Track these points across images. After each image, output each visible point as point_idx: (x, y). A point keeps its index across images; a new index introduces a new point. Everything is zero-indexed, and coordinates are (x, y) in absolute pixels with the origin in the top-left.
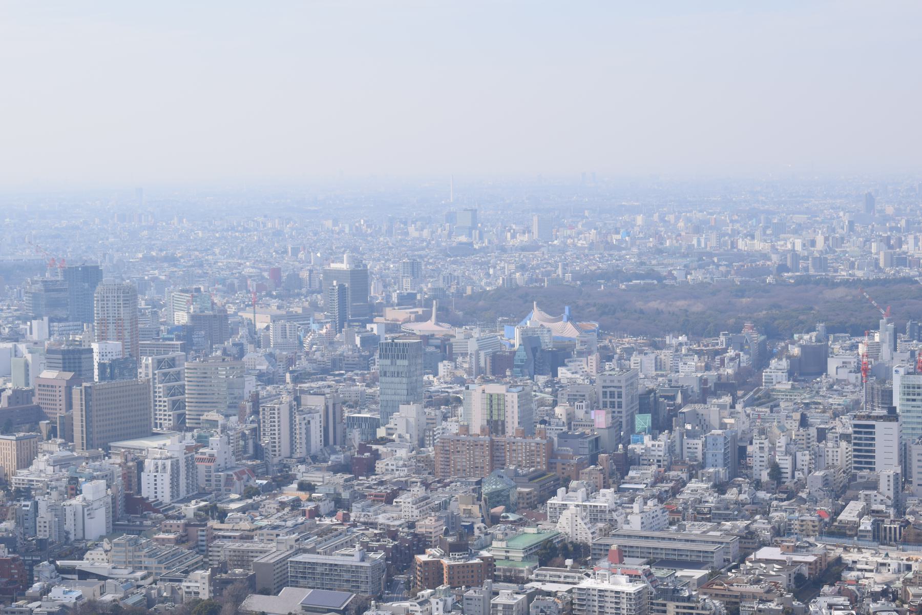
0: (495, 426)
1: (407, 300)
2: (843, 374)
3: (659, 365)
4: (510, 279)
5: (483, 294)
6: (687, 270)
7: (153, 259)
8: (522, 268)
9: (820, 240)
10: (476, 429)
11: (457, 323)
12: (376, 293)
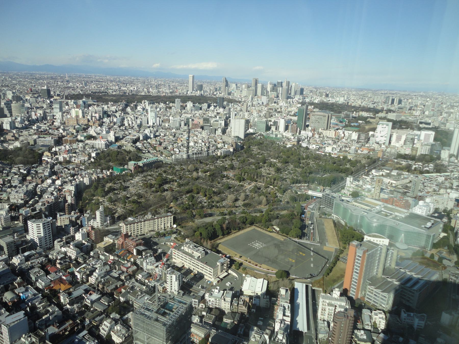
0: (77, 116)
1: (58, 95)
2: (140, 109)
3: (108, 107)
4: (79, 92)
5: (74, 95)
6: (113, 92)
7: (3, 86)
8: (82, 90)
9: (136, 89)
10: (73, 117)
11: (69, 99)
12: (52, 93)
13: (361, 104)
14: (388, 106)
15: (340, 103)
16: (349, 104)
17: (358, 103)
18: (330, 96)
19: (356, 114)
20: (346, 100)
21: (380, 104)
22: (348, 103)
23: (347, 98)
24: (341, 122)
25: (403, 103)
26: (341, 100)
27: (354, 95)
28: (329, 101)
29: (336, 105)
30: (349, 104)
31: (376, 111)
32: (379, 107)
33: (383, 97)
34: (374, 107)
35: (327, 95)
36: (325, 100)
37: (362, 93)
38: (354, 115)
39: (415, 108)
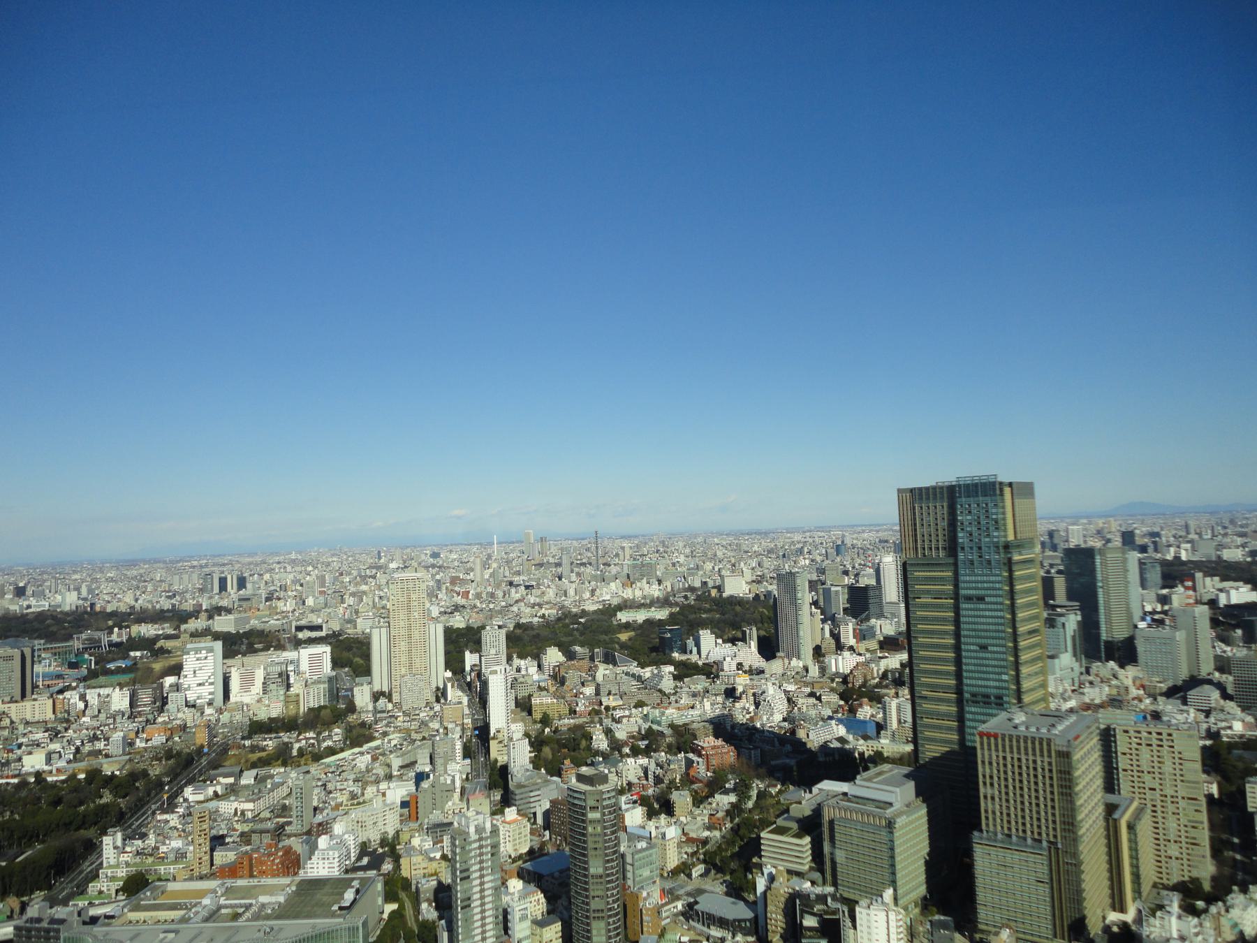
13: (133, 603)
14: (211, 598)
15: (67, 608)
16: (98, 608)
17: (126, 601)
18: (29, 591)
19: (119, 635)
20: (85, 599)
21: (188, 596)
22: (92, 605)
23: (90, 591)
24: (73, 666)
25: (249, 586)
26: (69, 601)
27: (112, 580)
28: (29, 607)
29: (54, 617)
30: (98, 608)
31: (179, 617)
32: (188, 605)
33: (195, 576)
34: (174, 605)
35: (20, 592)
36: (14, 608)
37: (135, 573)
38: (115, 638)
39: (282, 594)
